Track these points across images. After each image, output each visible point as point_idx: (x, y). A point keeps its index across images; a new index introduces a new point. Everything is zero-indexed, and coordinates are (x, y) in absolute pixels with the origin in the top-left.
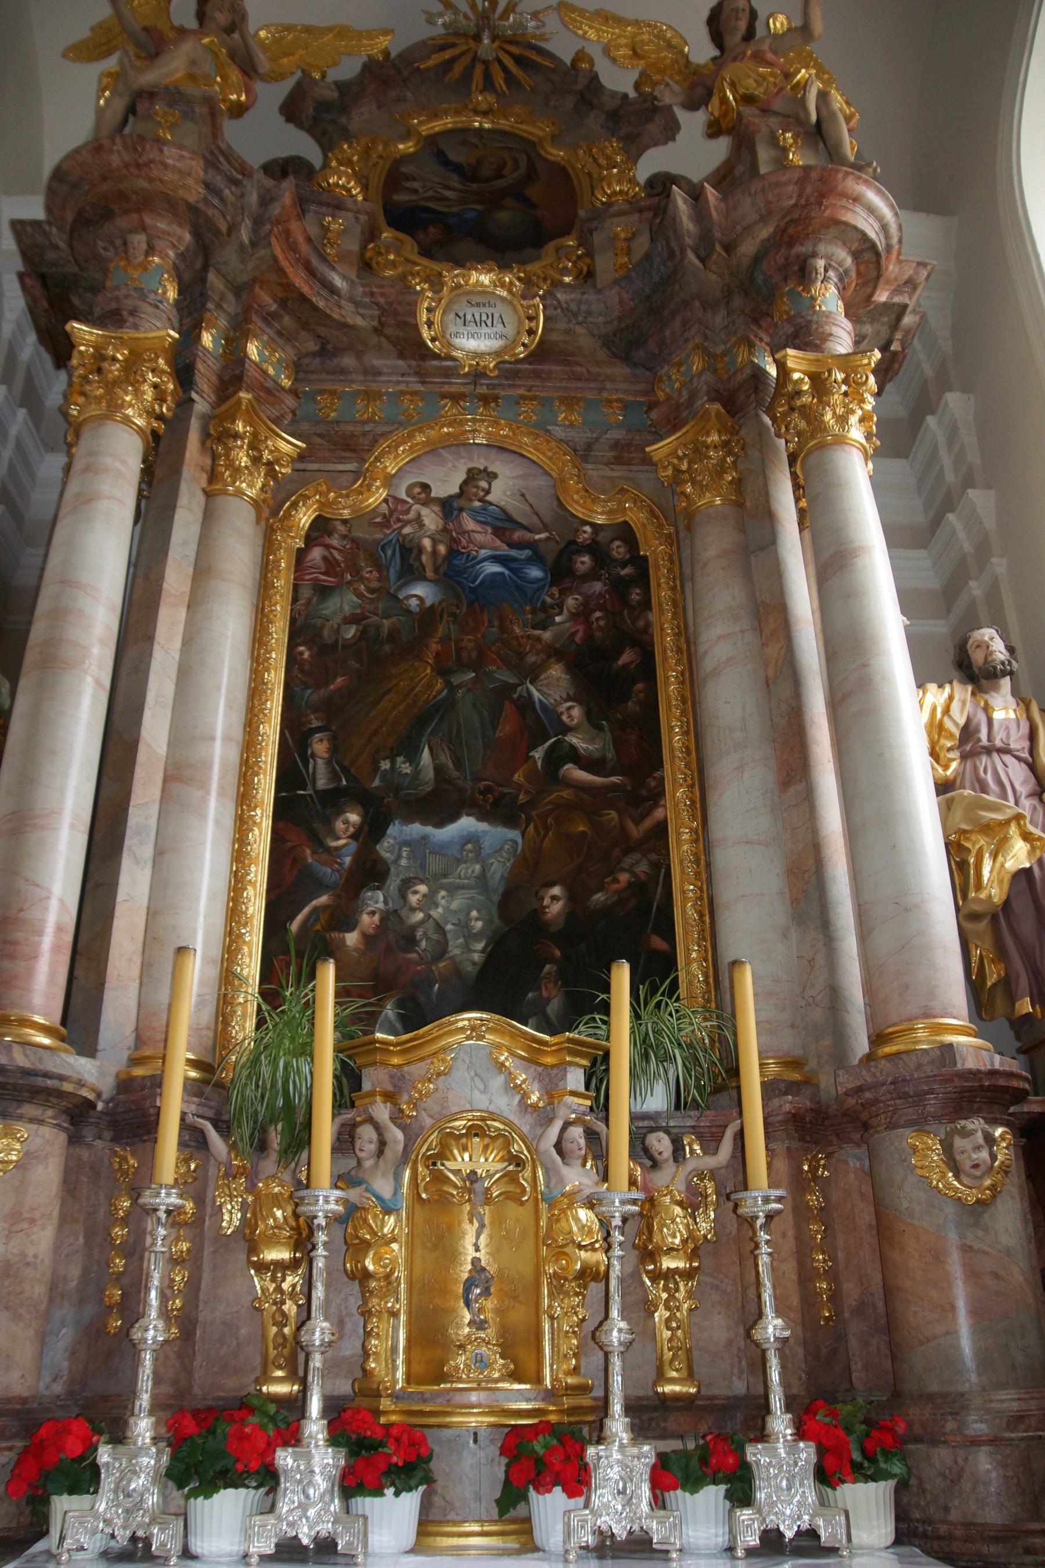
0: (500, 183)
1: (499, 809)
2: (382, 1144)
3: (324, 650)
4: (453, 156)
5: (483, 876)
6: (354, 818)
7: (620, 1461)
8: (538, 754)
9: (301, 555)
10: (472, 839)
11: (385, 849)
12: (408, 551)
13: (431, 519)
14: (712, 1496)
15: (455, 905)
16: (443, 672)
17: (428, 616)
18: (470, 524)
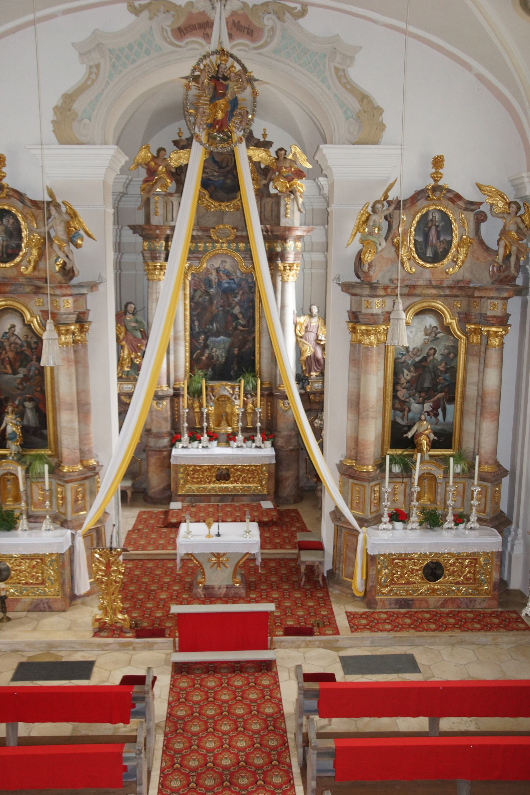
0: (228, 168)
1: (228, 335)
2: (211, 399)
3: (196, 303)
4: (217, 159)
5: (224, 348)
6: (203, 337)
7: (240, 437)
8: (234, 324)
9: (190, 282)
10: (224, 340)
11: (208, 342)
12: (210, 281)
13: (214, 273)
14: (250, 442)
15: (221, 351)
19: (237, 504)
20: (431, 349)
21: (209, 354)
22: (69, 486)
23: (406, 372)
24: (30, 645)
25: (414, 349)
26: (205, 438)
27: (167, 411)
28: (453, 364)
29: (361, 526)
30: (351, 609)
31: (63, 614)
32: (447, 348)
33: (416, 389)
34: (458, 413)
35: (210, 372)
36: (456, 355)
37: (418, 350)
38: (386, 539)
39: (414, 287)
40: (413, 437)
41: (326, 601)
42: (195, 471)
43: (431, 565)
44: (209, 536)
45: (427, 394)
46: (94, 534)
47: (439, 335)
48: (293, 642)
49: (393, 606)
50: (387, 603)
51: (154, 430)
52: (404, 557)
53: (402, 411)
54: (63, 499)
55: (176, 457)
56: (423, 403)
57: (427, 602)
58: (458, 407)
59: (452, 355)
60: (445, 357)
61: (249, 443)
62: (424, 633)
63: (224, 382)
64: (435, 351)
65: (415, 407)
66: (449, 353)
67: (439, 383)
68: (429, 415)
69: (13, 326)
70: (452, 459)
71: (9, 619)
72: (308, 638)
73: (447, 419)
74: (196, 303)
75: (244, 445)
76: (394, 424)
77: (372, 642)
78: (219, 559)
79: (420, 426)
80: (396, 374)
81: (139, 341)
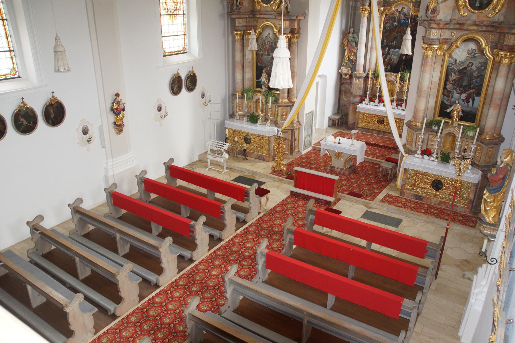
3: (386, 30)
12: (395, 18)
13: (398, 14)
16: (397, 33)
17: (396, 26)
18: (401, 15)
19: (385, 137)
20: (470, 63)
21: (390, 58)
22: (280, 108)
23: (453, 74)
24: (247, 170)
25: (460, 62)
26: (377, 101)
27: (360, 85)
28: (482, 74)
29: (406, 153)
30: (391, 193)
31: (267, 163)
32: (480, 63)
33: (458, 85)
34: (482, 103)
35: (389, 68)
36: (485, 68)
37: (462, 63)
38: (413, 162)
39: (462, 24)
40: (450, 112)
41: (383, 187)
42: (367, 116)
43: (436, 181)
44: (335, 142)
45: (464, 89)
46: (290, 132)
47: (476, 55)
48: (350, 199)
49: (413, 197)
50: (410, 195)
51: (354, 93)
52: (425, 174)
53: (448, 96)
54: (278, 113)
55: (359, 108)
56: (461, 94)
57: (431, 200)
58: (482, 99)
59: (483, 68)
60: (478, 68)
61: (399, 107)
62: (415, 212)
63: (392, 74)
64: (473, 64)
65: (456, 95)
66: (481, 66)
67: (472, 84)
68: (463, 101)
69: (269, 34)
70: (462, 127)
71: (247, 159)
72: (357, 199)
73: (474, 105)
74: (386, 30)
75: (396, 108)
76: (442, 103)
77: (387, 209)
78: (339, 155)
79: (455, 107)
80: (447, 75)
81: (353, 47)
